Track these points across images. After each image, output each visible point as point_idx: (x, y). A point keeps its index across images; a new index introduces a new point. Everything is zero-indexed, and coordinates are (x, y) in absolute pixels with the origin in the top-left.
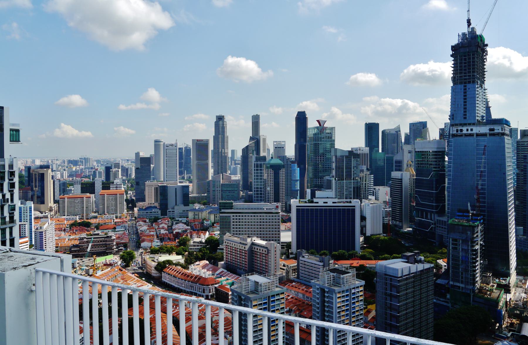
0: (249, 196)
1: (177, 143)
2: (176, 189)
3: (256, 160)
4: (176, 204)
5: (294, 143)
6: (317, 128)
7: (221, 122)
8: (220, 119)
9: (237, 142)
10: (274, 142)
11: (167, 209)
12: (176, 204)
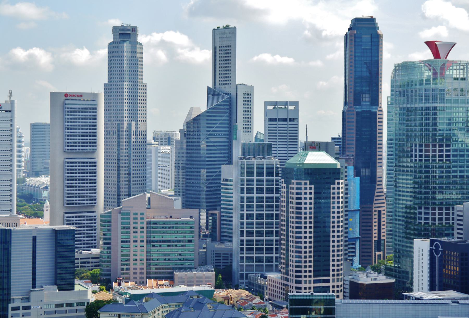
0: (218, 255)
1: (12, 103)
2: (34, 238)
3: (244, 154)
4: (34, 286)
5: (340, 106)
6: (428, 64)
7: (126, 46)
8: (125, 34)
9: (172, 101)
10: (267, 104)
11: (9, 301)
12: (34, 286)
